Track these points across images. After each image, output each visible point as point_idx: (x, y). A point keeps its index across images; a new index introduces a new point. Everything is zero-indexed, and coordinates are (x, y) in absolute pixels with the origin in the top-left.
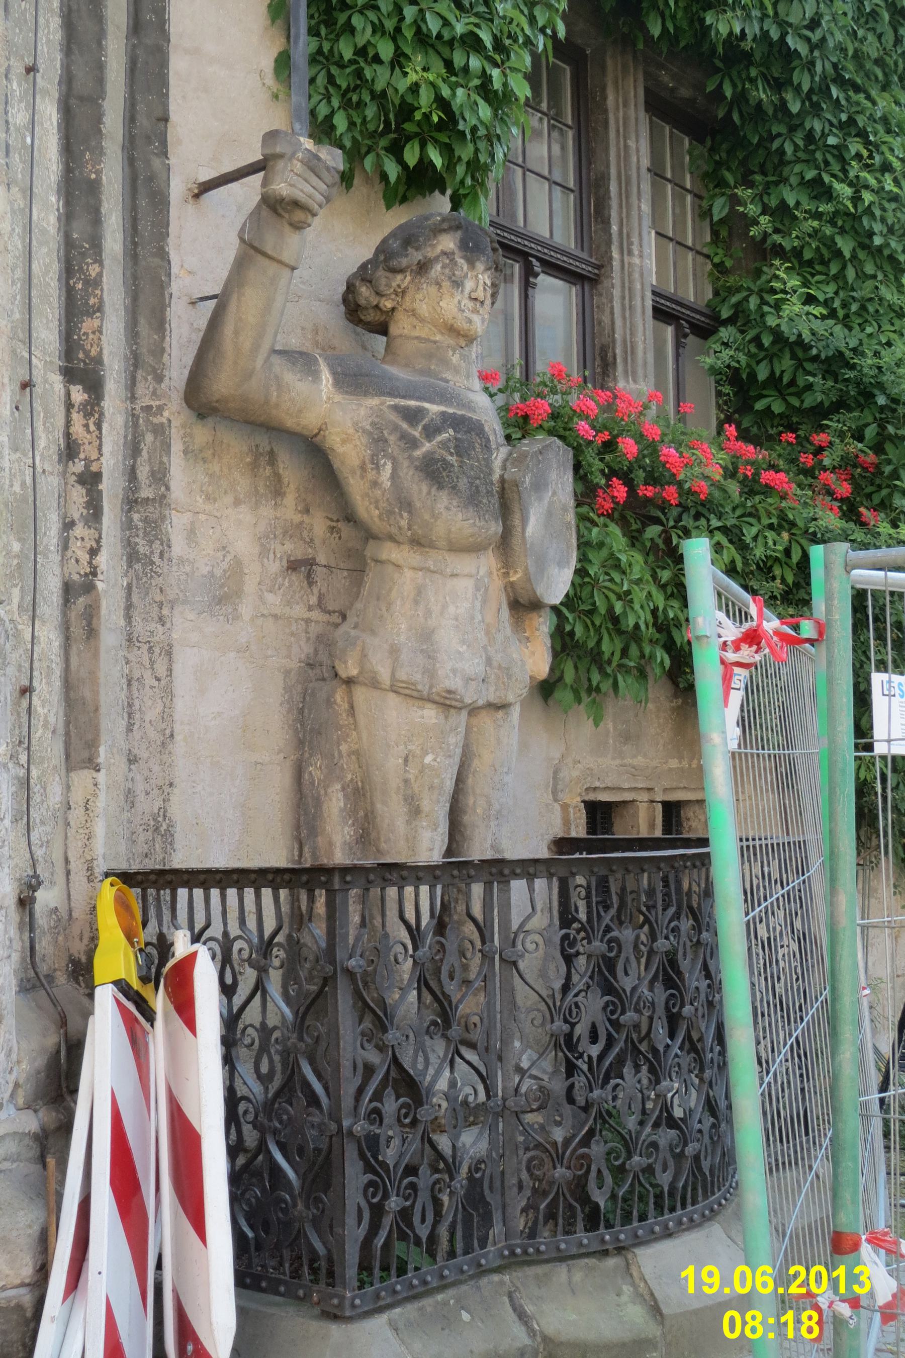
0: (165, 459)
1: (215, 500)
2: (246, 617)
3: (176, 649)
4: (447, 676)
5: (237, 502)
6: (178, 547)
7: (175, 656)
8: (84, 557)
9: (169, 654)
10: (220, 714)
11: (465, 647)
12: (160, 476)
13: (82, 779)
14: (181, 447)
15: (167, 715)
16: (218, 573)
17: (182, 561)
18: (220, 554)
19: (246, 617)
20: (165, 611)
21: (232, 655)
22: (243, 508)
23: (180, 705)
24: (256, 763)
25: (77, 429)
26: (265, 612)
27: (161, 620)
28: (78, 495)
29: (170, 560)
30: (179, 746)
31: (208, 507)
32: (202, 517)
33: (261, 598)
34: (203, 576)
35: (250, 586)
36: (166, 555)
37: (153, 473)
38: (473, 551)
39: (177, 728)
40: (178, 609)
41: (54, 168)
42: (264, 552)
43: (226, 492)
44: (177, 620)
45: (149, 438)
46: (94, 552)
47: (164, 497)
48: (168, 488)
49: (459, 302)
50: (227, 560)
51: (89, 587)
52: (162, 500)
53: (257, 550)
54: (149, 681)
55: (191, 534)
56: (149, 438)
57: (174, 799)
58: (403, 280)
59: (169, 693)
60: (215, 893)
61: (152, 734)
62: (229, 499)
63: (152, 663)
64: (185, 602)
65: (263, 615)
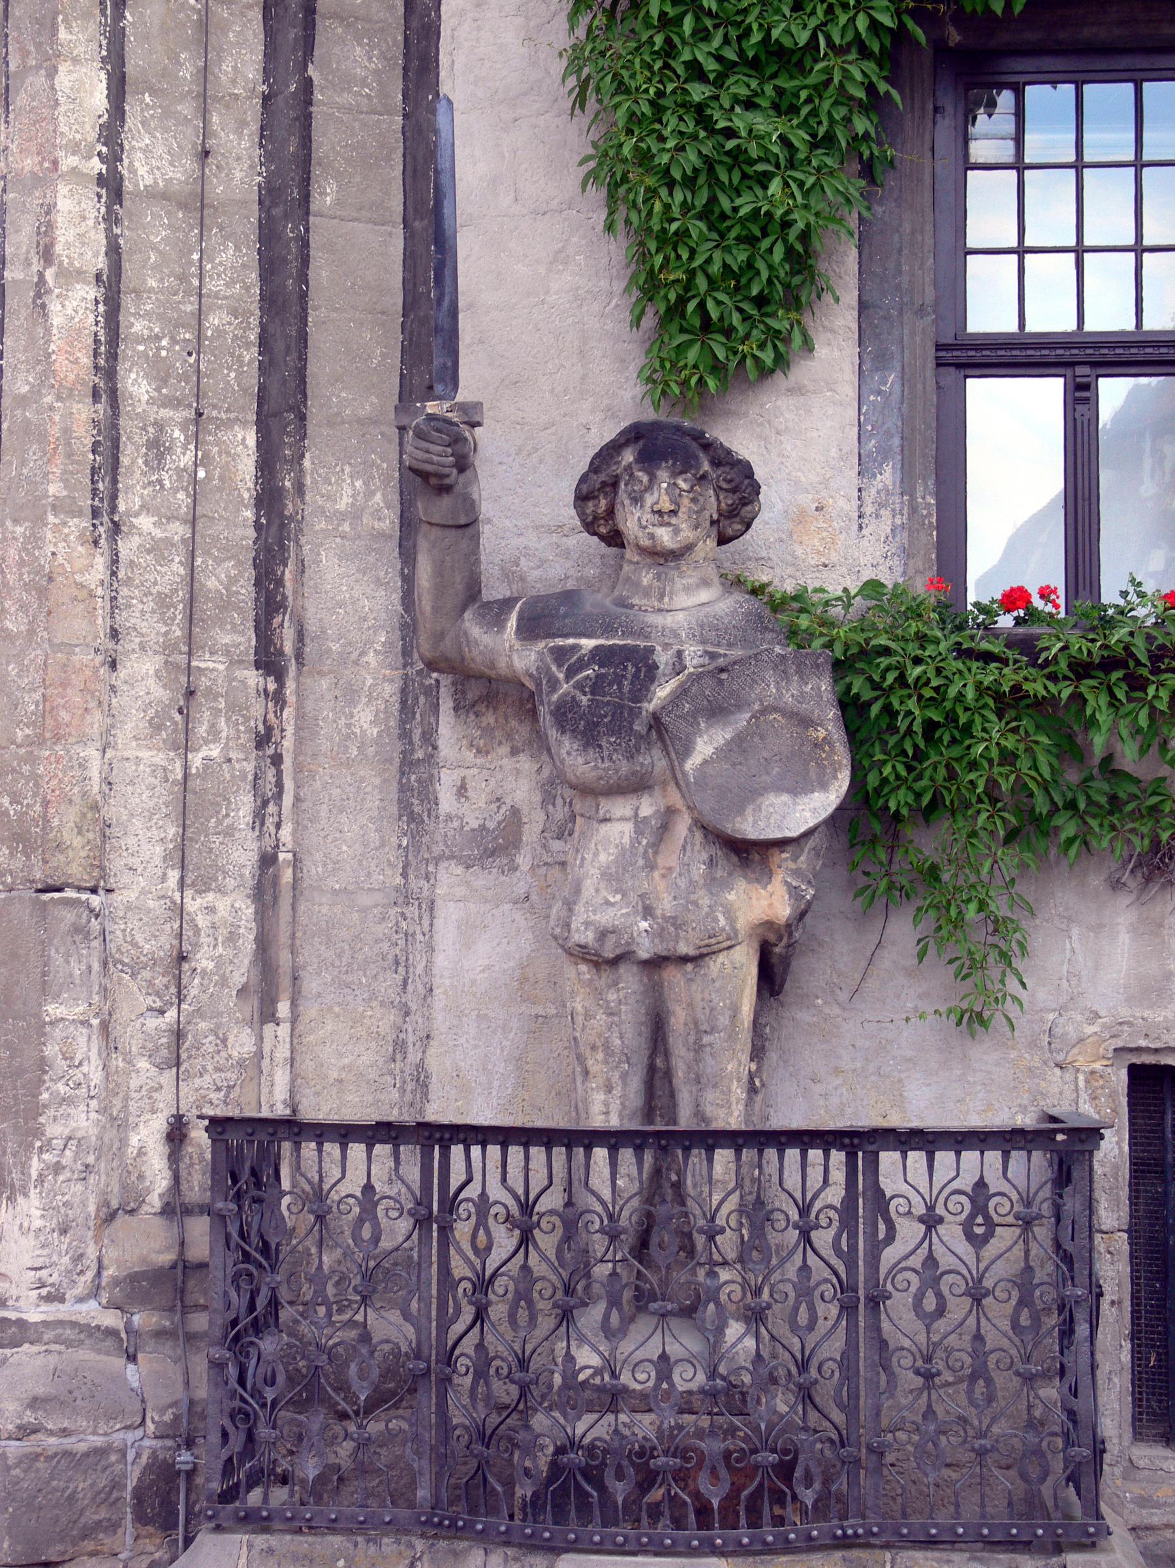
0: (432, 720)
1: (487, 753)
3: (439, 903)
4: (578, 930)
5: (514, 752)
6: (447, 802)
7: (437, 913)
8: (273, 830)
9: (432, 909)
10: (488, 968)
11: (618, 897)
12: (430, 737)
13: (269, 1029)
14: (451, 704)
15: (428, 970)
16: (491, 825)
17: (449, 818)
18: (494, 806)
20: (431, 869)
21: (507, 907)
22: (523, 757)
23: (441, 961)
24: (537, 1016)
25: (271, 716)
26: (550, 860)
27: (428, 880)
28: (271, 773)
29: (437, 817)
30: (439, 1000)
31: (480, 761)
33: (544, 846)
34: (473, 830)
35: (531, 833)
36: (433, 814)
37: (424, 733)
38: (635, 791)
39: (437, 981)
40: (443, 865)
42: (548, 799)
43: (500, 743)
44: (442, 875)
45: (422, 700)
46: (278, 826)
48: (435, 748)
49: (639, 519)
50: (502, 811)
51: (274, 858)
52: (430, 759)
53: (537, 798)
54: (420, 937)
55: (462, 790)
56: (422, 700)
57: (431, 1051)
58: (596, 506)
59: (431, 949)
60: (580, 1152)
61: (420, 988)
62: (505, 749)
63: (420, 918)
65: (546, 864)
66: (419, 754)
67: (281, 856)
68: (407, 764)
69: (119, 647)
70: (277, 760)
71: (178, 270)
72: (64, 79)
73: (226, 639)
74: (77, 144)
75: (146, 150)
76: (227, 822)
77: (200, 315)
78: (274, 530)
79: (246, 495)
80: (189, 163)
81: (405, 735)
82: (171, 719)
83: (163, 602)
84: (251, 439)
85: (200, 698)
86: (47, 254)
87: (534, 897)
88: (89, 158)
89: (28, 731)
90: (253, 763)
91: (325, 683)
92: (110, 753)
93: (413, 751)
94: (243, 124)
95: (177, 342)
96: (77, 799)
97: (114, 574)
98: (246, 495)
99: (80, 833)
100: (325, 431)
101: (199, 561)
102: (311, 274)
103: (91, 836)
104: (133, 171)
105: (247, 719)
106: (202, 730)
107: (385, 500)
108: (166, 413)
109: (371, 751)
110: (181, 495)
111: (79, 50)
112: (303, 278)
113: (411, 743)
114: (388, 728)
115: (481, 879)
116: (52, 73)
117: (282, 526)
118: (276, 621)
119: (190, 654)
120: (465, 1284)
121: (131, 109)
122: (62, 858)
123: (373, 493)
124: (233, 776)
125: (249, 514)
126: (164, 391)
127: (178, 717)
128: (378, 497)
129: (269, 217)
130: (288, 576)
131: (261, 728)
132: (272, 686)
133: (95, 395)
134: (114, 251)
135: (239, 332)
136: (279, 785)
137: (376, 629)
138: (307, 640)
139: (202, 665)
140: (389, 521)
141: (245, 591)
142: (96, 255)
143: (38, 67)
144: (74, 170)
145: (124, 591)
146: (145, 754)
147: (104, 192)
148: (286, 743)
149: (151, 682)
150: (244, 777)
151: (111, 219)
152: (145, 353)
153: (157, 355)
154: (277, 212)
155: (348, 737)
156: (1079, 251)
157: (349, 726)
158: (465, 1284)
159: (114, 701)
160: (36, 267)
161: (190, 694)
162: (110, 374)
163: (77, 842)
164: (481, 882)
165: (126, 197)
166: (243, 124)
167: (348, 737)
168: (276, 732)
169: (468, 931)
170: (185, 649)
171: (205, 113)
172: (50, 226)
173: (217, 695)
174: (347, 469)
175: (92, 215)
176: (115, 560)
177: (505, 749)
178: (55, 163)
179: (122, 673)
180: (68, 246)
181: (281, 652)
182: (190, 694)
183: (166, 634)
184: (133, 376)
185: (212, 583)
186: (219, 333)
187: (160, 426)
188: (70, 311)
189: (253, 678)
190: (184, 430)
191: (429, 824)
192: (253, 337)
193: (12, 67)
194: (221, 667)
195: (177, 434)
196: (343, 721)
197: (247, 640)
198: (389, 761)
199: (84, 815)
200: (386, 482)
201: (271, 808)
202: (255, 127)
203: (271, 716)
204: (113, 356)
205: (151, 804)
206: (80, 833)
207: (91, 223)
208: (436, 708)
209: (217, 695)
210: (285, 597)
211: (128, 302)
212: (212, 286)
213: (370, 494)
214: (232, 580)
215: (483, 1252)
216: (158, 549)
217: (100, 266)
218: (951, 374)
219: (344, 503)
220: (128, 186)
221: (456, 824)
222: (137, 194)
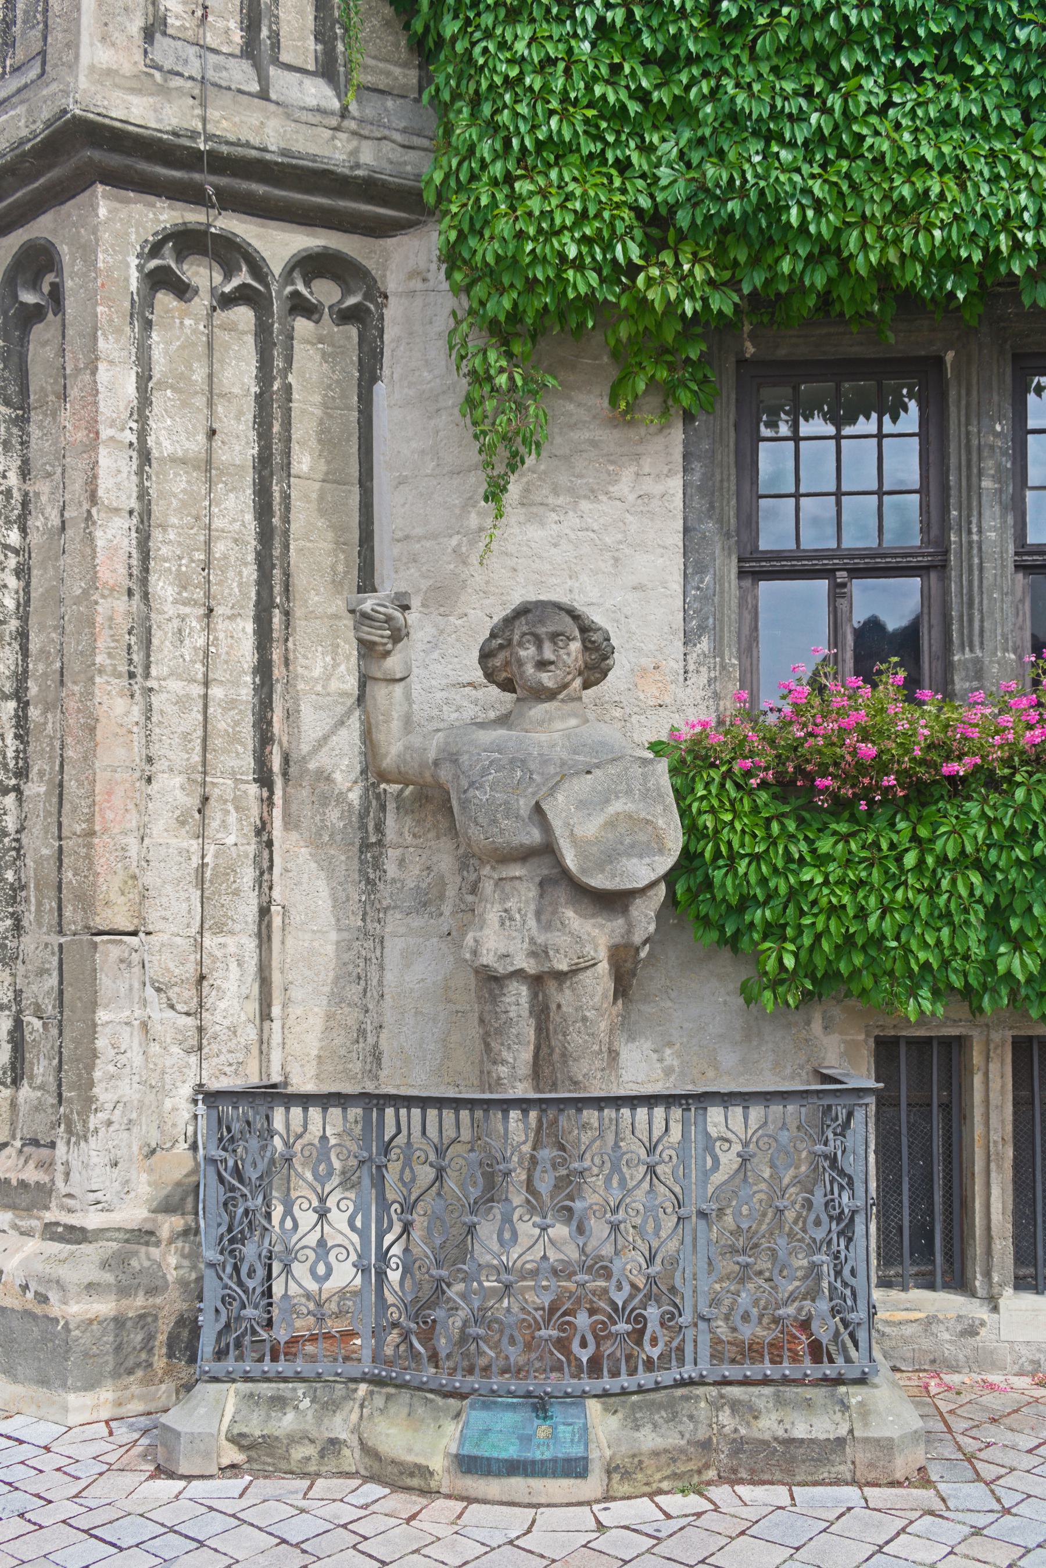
2: (447, 913)
12: (379, 828)
16: (424, 886)
17: (394, 881)
18: (425, 873)
19: (447, 913)
25: (265, 814)
28: (266, 854)
32: (411, 850)
41: (249, 659)
47: (380, 841)
51: (268, 910)
52: (380, 843)
55: (402, 863)
62: (431, 835)
64: (395, 908)
66: (373, 840)
67: (273, 908)
68: (365, 846)
69: (153, 769)
70: (270, 844)
71: (194, 512)
72: (103, 374)
73: (232, 762)
74: (113, 421)
75: (168, 430)
76: (234, 886)
77: (208, 543)
78: (265, 690)
79: (246, 666)
80: (201, 438)
81: (363, 827)
82: (192, 817)
83: (186, 736)
84: (250, 627)
85: (212, 802)
86: (93, 498)
87: (454, 933)
88: (123, 430)
89: (84, 826)
90: (254, 847)
91: (305, 793)
92: (147, 841)
93: (367, 838)
94: (240, 413)
95: (193, 561)
96: (121, 872)
97: (148, 718)
98: (246, 666)
99: (123, 894)
100: (303, 623)
101: (211, 710)
102: (292, 516)
103: (131, 896)
104: (158, 443)
105: (248, 817)
106: (215, 824)
107: (348, 670)
108: (187, 610)
109: (338, 838)
110: (199, 665)
111: (115, 355)
112: (286, 520)
113: (367, 832)
114: (351, 822)
115: (417, 922)
116: (94, 372)
117: (272, 685)
118: (267, 751)
119: (205, 773)
120: (396, 1206)
121: (157, 398)
122: (109, 911)
123: (339, 665)
124: (239, 856)
125: (249, 679)
126: (185, 594)
127: (197, 816)
128: (343, 668)
129: (260, 477)
130: (275, 719)
131: (258, 822)
132: (265, 794)
133: (130, 593)
134: (143, 494)
135: (240, 556)
136: (271, 860)
137: (341, 756)
138: (291, 763)
139: (215, 780)
140: (351, 684)
141: (247, 731)
142: (129, 498)
143: (86, 368)
144: (112, 438)
145: (157, 730)
146: (173, 841)
147: (135, 454)
148: (275, 833)
149: (178, 793)
150: (247, 856)
151: (140, 472)
152: (170, 569)
153: (179, 570)
154: (266, 473)
155: (322, 828)
156: (838, 494)
157: (322, 821)
158: (396, 1206)
159: (150, 805)
160: (86, 506)
161: (205, 799)
162: (144, 582)
163: (121, 900)
164: (416, 924)
165: (153, 461)
166: (240, 413)
167: (322, 828)
168: (268, 826)
169: (408, 958)
170: (200, 769)
171: (210, 404)
172: (95, 477)
173: (226, 801)
174: (320, 649)
175: (125, 470)
176: (149, 709)
177: (431, 835)
178: (97, 433)
179: (155, 786)
180: (108, 491)
181: (271, 771)
182: (205, 799)
183: (188, 759)
184: (161, 584)
185: (222, 726)
186: (225, 557)
187: (183, 618)
188: (110, 537)
189: (253, 789)
190: (199, 619)
191: (381, 886)
192: (251, 557)
193: (68, 371)
194: (229, 782)
195: (194, 624)
196: (318, 817)
197: (248, 762)
198: (352, 844)
199: (126, 882)
200: (348, 658)
201: (266, 877)
202: (250, 417)
203: (265, 814)
204: (146, 570)
205: (179, 874)
206: (123, 894)
207: (125, 475)
208: (383, 808)
209: (226, 801)
210: (273, 734)
211: (157, 534)
212: (217, 523)
213: (336, 666)
214: (237, 723)
215: (409, 1185)
216: (182, 703)
217: (133, 505)
218: (747, 583)
219: (317, 672)
220: (155, 453)
221: (399, 885)
222: (161, 460)
